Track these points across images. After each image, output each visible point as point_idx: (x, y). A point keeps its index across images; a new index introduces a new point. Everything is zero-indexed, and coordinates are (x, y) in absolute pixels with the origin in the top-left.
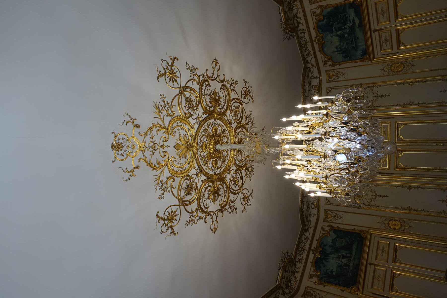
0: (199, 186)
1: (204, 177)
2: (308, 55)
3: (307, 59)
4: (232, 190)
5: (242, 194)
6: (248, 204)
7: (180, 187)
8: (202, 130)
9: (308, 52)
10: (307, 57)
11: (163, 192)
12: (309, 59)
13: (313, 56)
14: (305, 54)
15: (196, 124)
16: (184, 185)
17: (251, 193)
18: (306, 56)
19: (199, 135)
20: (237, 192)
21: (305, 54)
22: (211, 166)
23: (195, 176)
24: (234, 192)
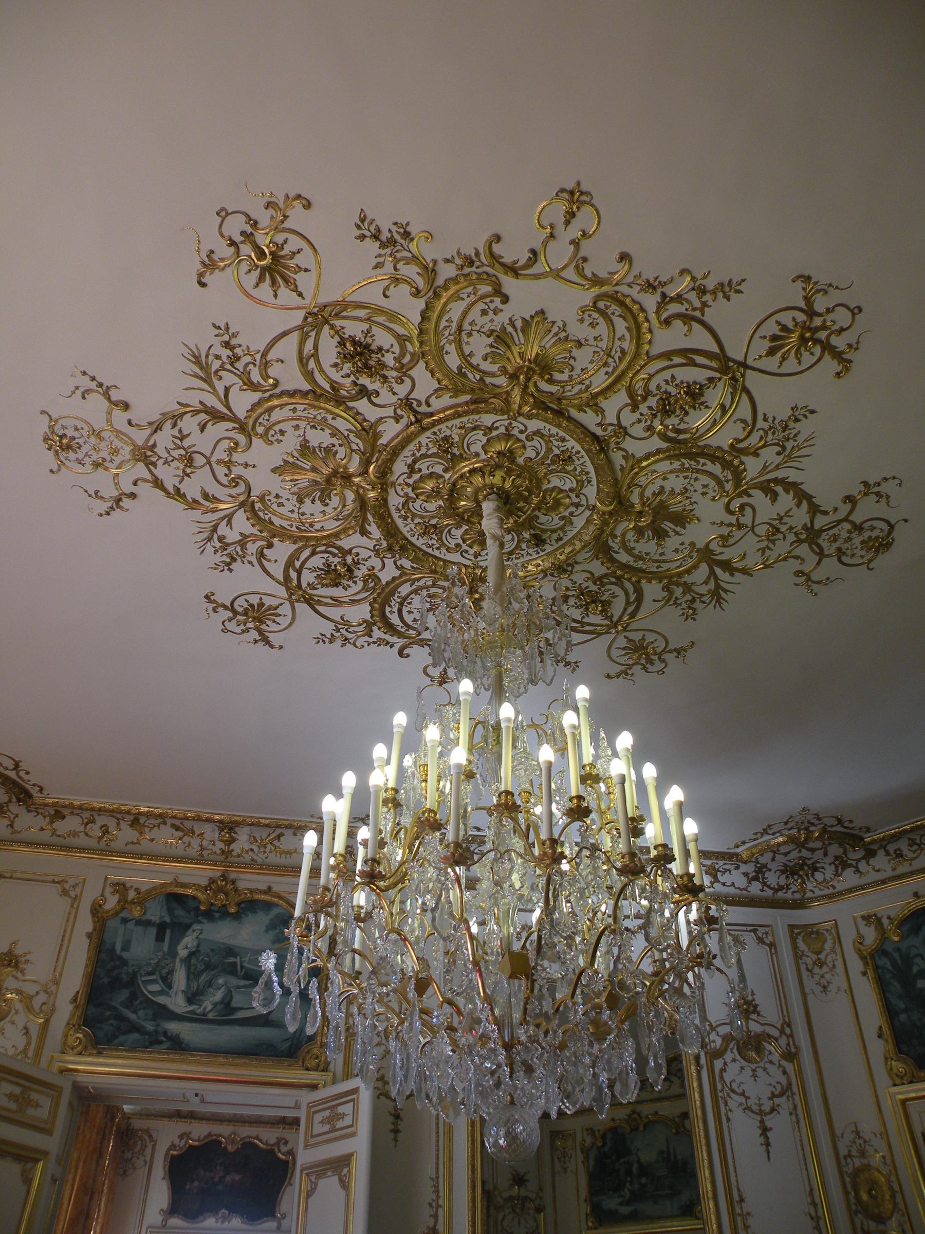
0: (362, 405)
1: (390, 431)
2: (899, 855)
3: (881, 853)
4: (306, 553)
5: (274, 602)
6: (231, 626)
7: (381, 319)
8: (572, 444)
9: (910, 855)
10: (888, 853)
11: (385, 235)
12: (880, 860)
13: (890, 873)
14: (903, 845)
15: (598, 420)
16: (382, 339)
17: (267, 642)
18: (891, 848)
19: (554, 430)
20: (294, 575)
21: (903, 845)
22: (425, 471)
23: (402, 390)
24: (298, 564)
